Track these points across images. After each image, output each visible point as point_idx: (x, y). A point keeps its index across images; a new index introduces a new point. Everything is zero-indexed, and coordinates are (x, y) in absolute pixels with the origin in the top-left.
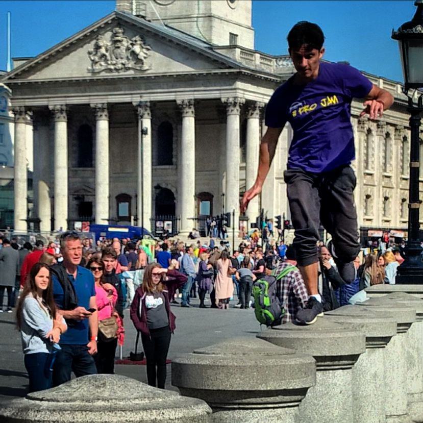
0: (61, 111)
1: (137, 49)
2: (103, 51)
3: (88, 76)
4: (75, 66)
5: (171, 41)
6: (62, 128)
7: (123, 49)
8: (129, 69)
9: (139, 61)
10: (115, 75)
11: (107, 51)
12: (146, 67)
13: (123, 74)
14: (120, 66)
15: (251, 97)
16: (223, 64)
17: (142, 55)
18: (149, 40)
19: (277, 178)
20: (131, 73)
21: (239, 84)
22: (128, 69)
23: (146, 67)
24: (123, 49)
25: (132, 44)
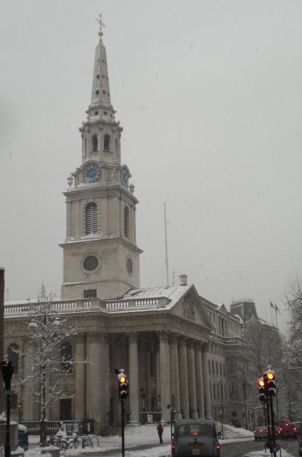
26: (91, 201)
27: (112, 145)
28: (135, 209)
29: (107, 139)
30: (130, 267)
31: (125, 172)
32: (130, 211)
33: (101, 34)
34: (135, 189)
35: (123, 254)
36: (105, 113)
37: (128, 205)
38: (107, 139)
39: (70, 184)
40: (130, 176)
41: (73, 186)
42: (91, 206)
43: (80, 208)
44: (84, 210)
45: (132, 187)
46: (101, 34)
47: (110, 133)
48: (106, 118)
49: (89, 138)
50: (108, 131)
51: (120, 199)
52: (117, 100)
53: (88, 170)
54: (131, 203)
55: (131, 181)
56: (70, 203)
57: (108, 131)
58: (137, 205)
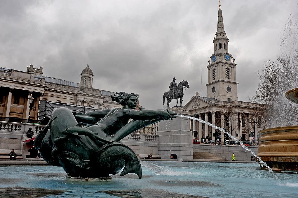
13: (196, 108)
18: (200, 101)
21: (214, 108)
26: (214, 68)
27: (223, 46)
28: (234, 68)
29: (220, 45)
30: (229, 89)
31: (229, 56)
33: (220, 6)
35: (226, 85)
36: (220, 35)
37: (228, 67)
38: (220, 45)
39: (209, 63)
45: (234, 60)
46: (220, 6)
48: (220, 37)
50: (220, 42)
52: (226, 30)
53: (213, 57)
54: (232, 66)
56: (209, 70)
57: (220, 42)
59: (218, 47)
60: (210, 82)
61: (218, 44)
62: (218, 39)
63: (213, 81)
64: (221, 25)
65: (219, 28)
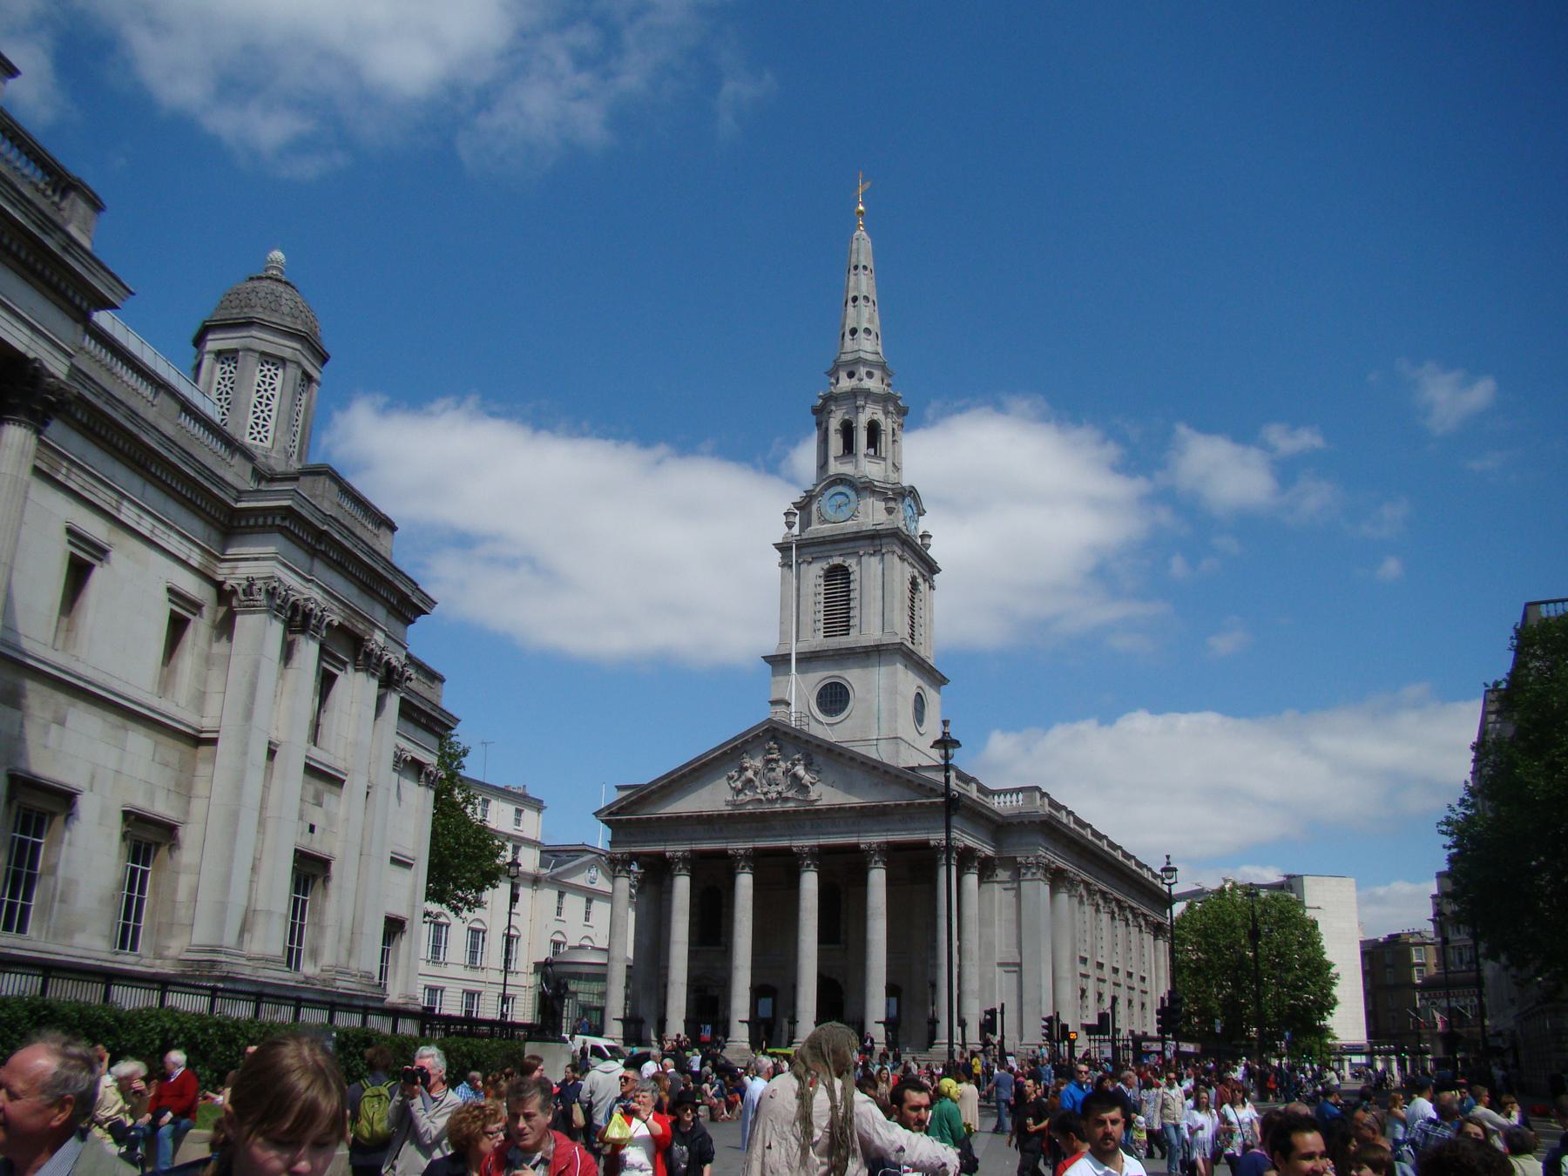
0: (684, 859)
1: (800, 770)
2: (750, 774)
3: (726, 809)
4: (712, 798)
5: (852, 759)
6: (682, 885)
7: (780, 771)
8: (786, 799)
9: (804, 788)
10: (767, 808)
11: (756, 774)
12: (813, 796)
13: (778, 807)
14: (775, 795)
15: (970, 842)
16: (932, 790)
17: (807, 778)
18: (819, 759)
19: (1001, 965)
20: (791, 806)
22: (786, 799)
23: (813, 796)
24: (780, 771)
25: (794, 765)
26: (837, 560)
28: (932, 587)
29: (874, 430)
32: (921, 587)
34: (932, 541)
36: (870, 375)
38: (874, 430)
39: (790, 525)
40: (921, 513)
41: (796, 530)
42: (838, 576)
43: (814, 572)
44: (821, 581)
47: (880, 416)
48: (874, 385)
49: (834, 423)
51: (900, 558)
55: (924, 525)
58: (936, 577)
59: (862, 438)
60: (805, 647)
61: (863, 420)
62: (868, 394)
63: (817, 640)
64: (871, 321)
65: (861, 335)
